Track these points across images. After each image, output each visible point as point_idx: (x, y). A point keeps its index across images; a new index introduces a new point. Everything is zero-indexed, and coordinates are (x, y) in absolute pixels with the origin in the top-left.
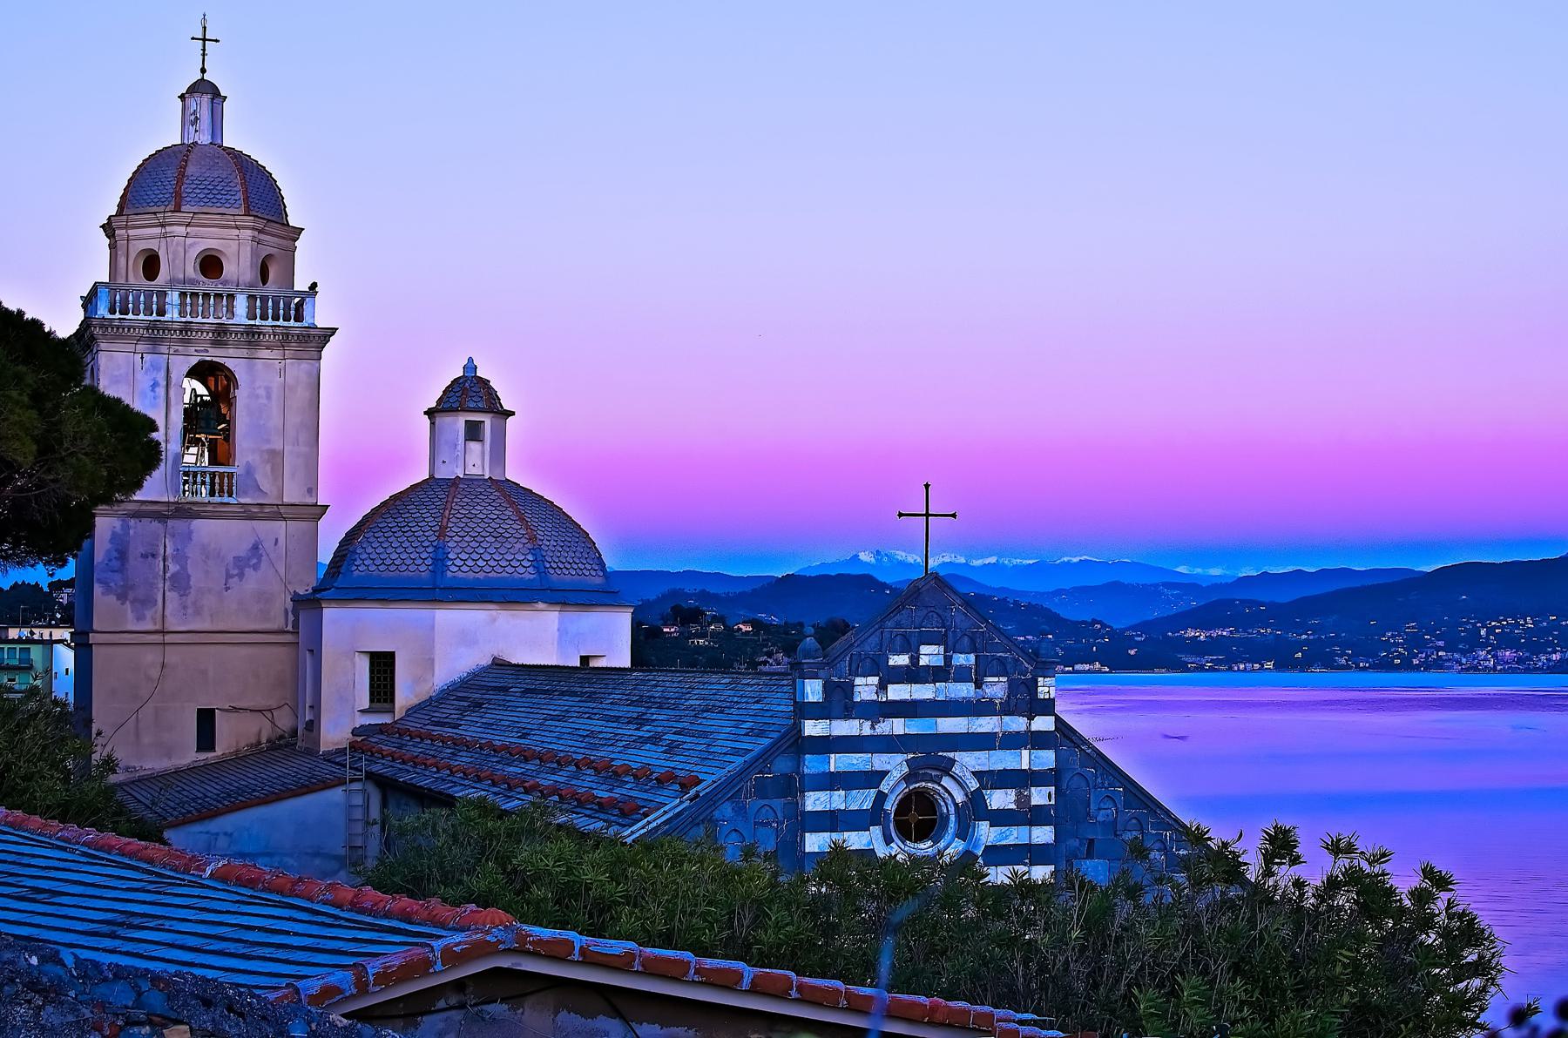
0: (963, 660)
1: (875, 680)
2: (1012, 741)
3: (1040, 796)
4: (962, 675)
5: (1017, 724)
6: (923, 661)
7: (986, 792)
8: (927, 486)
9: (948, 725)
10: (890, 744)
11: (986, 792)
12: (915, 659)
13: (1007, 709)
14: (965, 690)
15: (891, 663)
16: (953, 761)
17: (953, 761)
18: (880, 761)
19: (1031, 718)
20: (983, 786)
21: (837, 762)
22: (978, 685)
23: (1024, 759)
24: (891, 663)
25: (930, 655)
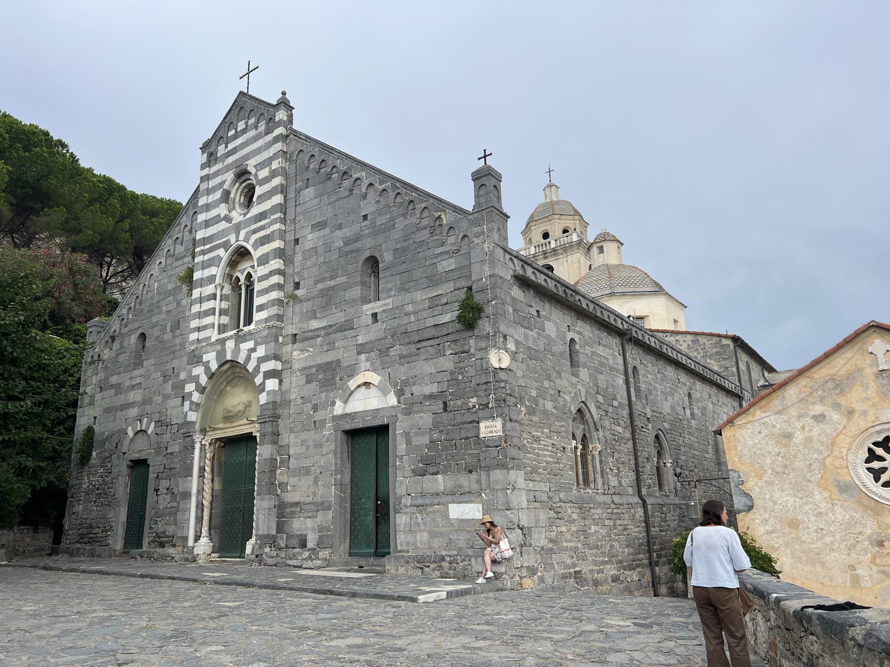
2: (268, 146)
3: (275, 165)
10: (227, 169)
16: (247, 165)
17: (247, 165)
20: (257, 171)
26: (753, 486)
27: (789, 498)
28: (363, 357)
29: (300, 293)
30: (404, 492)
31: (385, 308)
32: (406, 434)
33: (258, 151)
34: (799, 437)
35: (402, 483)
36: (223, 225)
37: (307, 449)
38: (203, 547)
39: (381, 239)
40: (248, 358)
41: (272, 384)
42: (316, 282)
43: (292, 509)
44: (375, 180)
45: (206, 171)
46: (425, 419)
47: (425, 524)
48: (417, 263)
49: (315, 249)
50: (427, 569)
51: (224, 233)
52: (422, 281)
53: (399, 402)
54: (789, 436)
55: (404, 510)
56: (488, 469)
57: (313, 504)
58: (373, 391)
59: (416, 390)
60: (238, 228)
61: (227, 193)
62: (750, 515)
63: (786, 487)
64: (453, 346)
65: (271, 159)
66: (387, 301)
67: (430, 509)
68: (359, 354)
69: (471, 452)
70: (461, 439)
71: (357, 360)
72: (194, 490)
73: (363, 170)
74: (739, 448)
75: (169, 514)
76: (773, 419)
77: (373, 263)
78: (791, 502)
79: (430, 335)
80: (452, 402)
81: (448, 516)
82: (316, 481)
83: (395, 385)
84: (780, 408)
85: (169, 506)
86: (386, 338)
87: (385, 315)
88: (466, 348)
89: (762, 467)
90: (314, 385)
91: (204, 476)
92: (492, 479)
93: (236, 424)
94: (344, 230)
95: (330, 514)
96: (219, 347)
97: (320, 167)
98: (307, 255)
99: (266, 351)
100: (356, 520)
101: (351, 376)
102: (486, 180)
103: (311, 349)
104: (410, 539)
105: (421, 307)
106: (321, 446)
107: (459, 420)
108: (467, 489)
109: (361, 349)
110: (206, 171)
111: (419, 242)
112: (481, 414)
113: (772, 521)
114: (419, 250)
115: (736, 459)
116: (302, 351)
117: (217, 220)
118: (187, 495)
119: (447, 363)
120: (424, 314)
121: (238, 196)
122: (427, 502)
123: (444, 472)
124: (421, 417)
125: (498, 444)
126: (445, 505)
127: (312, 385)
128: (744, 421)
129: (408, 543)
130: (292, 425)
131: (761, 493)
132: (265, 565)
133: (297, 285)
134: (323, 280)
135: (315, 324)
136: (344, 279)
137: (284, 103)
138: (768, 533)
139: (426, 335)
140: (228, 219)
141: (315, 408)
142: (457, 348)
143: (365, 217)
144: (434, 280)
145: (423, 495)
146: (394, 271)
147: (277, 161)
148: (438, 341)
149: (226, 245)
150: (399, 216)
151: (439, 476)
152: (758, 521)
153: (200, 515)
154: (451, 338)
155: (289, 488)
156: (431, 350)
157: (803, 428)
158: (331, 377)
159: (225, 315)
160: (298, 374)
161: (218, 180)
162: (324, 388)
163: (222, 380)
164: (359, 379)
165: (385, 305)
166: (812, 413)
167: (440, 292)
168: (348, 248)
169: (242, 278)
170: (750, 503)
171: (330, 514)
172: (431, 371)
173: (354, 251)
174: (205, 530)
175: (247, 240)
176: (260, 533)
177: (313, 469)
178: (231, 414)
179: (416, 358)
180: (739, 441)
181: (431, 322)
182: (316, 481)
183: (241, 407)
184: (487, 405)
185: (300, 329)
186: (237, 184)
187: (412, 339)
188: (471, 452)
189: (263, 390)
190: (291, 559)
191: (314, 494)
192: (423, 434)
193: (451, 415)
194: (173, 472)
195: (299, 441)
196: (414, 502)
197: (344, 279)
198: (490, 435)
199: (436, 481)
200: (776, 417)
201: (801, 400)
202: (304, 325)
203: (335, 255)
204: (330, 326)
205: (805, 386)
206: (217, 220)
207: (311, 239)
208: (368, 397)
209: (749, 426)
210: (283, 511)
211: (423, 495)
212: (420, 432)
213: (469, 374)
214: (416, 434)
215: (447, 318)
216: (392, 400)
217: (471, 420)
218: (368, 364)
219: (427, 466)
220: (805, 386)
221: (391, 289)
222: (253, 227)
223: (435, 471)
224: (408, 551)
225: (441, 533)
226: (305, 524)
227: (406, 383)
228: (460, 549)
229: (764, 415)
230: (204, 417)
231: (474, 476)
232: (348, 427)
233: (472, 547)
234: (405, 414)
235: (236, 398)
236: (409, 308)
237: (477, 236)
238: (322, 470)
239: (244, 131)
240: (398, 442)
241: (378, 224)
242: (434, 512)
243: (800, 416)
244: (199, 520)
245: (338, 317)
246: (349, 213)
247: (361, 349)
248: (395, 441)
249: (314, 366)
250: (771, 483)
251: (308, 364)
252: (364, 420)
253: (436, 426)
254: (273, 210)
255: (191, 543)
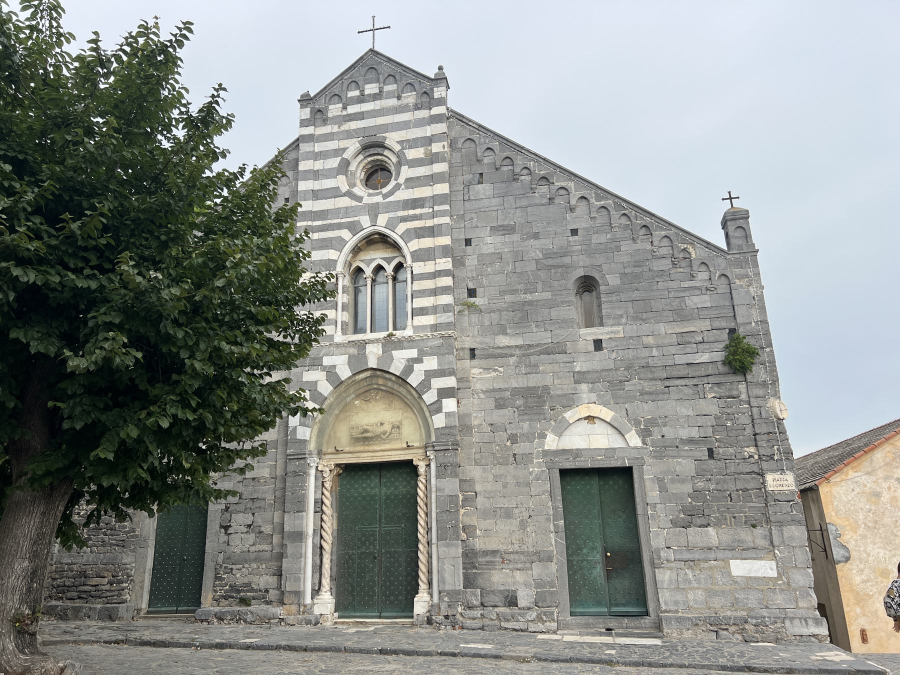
0: (390, 88)
1: (341, 105)
2: (420, 123)
3: (436, 148)
4: (390, 95)
5: (423, 114)
6: (366, 92)
7: (406, 151)
8: (374, 17)
9: (380, 121)
11: (406, 151)
12: (362, 92)
13: (417, 107)
14: (392, 102)
15: (349, 96)
16: (385, 138)
17: (385, 138)
18: (343, 144)
19: (430, 109)
20: (403, 148)
21: (318, 147)
22: (399, 98)
23: (429, 131)
24: (349, 96)
25: (371, 89)
26: (849, 538)
27: (880, 550)
28: (584, 387)
29: (478, 301)
30: (662, 545)
31: (613, 336)
32: (660, 481)
33: (405, 125)
34: (886, 497)
35: (657, 534)
36: (345, 202)
37: (505, 486)
38: (325, 604)
39: (600, 260)
40: (409, 369)
41: (449, 405)
42: (503, 293)
43: (488, 559)
44: (591, 195)
45: (309, 130)
46: (685, 465)
47: (698, 581)
48: (656, 293)
49: (499, 256)
50: (725, 632)
51: (347, 211)
52: (665, 314)
53: (644, 443)
54: (878, 495)
55: (666, 564)
56: (781, 524)
57: (522, 553)
58: (599, 426)
59: (669, 432)
60: (374, 211)
61: (346, 164)
62: (848, 565)
63: (877, 540)
64: (716, 389)
65: (430, 140)
66: (615, 328)
67: (706, 565)
68: (577, 382)
69: (752, 505)
70: (737, 490)
71: (575, 389)
72: (310, 531)
73: (571, 180)
74: (835, 503)
75: (256, 560)
76: (864, 479)
77: (588, 285)
78: (882, 554)
79: (682, 373)
80: (721, 450)
81: (730, 573)
82: (523, 525)
83: (637, 423)
84: (869, 469)
85: (253, 549)
86: (617, 369)
87: (613, 344)
88: (735, 393)
89: (856, 522)
90: (508, 412)
91: (323, 512)
92: (786, 535)
93: (371, 448)
94: (542, 241)
95: (553, 567)
96: (353, 351)
97: (491, 160)
98: (482, 259)
99: (439, 364)
100: (575, 573)
101: (568, 406)
102: (735, 221)
103: (501, 369)
104: (679, 597)
105: (666, 341)
106: (528, 485)
107: (732, 469)
108: (752, 545)
109: (580, 378)
110: (309, 130)
111: (658, 271)
112: (765, 465)
113: (867, 571)
114: (657, 280)
115: (833, 513)
116: (487, 369)
117: (335, 193)
118: (299, 536)
119: (710, 406)
120: (673, 350)
121: (359, 171)
122: (697, 556)
123: (718, 524)
124: (680, 463)
125: (790, 499)
126: (726, 561)
127: (506, 411)
128: (838, 479)
129: (676, 603)
130: (478, 456)
131: (856, 546)
132: (463, 628)
133: (472, 293)
134: (514, 292)
135: (503, 341)
136: (547, 295)
137: (441, 79)
138: (864, 582)
139: (675, 373)
140: (349, 194)
141: (513, 439)
142: (723, 391)
143: (574, 232)
144: (681, 315)
145: (689, 549)
146: (623, 297)
147: (440, 144)
148: (695, 381)
149: (354, 228)
150: (626, 239)
151: (710, 529)
152: (854, 571)
153: (318, 562)
154: (712, 379)
155: (478, 532)
156: (686, 390)
157: (889, 488)
158: (538, 404)
159: (347, 311)
160: (482, 396)
161: (332, 145)
162: (526, 417)
163: (351, 390)
164: (583, 411)
165: (614, 332)
166: (896, 476)
167: (693, 329)
168: (550, 262)
169: (368, 271)
170: (846, 555)
171: (553, 567)
172: (689, 414)
173: (559, 267)
174: (326, 582)
175: (391, 225)
176: (448, 587)
177: (517, 511)
178: (369, 435)
179: (666, 397)
180: (835, 497)
181: (681, 359)
182: (523, 525)
183: (387, 427)
184: (771, 457)
185: (481, 343)
186: (361, 157)
187: (656, 375)
188: (752, 505)
189: (439, 410)
190: (508, 621)
191: (522, 541)
192: (683, 481)
193: (721, 464)
194: (257, 504)
195: (491, 477)
196: (678, 557)
197: (547, 295)
198: (781, 488)
199: (707, 533)
200: (866, 477)
201: (887, 464)
202: (487, 340)
203: (532, 266)
204: (530, 346)
205: (889, 452)
206: (335, 193)
207: (489, 243)
208: (591, 433)
209: (843, 483)
210: (472, 561)
211: (689, 549)
212: (679, 479)
213: (741, 421)
214: (673, 481)
215: (705, 358)
216: (634, 440)
217: (748, 470)
218: (593, 397)
219: (692, 516)
220: (889, 452)
221: (621, 316)
222: (402, 213)
223: (705, 523)
224: (677, 612)
225: (723, 592)
226: (513, 577)
227: (653, 422)
228: (752, 610)
229: (856, 474)
230: (321, 433)
231: (759, 531)
232: (568, 465)
233: (767, 607)
234: (655, 457)
235: (376, 415)
236: (650, 340)
237: (741, 277)
238: (532, 513)
239: (375, 97)
240: (648, 489)
241: (594, 241)
242: (711, 568)
243: (886, 478)
244: (318, 568)
245: (544, 337)
246: (548, 224)
247: (580, 378)
248: (643, 487)
249: (506, 390)
250: (864, 537)
251: (496, 386)
252: (594, 460)
253: (700, 474)
254: (436, 199)
255: (308, 601)
